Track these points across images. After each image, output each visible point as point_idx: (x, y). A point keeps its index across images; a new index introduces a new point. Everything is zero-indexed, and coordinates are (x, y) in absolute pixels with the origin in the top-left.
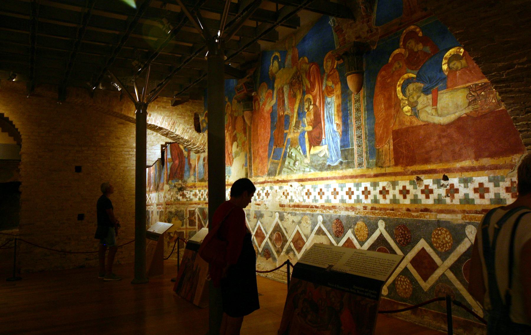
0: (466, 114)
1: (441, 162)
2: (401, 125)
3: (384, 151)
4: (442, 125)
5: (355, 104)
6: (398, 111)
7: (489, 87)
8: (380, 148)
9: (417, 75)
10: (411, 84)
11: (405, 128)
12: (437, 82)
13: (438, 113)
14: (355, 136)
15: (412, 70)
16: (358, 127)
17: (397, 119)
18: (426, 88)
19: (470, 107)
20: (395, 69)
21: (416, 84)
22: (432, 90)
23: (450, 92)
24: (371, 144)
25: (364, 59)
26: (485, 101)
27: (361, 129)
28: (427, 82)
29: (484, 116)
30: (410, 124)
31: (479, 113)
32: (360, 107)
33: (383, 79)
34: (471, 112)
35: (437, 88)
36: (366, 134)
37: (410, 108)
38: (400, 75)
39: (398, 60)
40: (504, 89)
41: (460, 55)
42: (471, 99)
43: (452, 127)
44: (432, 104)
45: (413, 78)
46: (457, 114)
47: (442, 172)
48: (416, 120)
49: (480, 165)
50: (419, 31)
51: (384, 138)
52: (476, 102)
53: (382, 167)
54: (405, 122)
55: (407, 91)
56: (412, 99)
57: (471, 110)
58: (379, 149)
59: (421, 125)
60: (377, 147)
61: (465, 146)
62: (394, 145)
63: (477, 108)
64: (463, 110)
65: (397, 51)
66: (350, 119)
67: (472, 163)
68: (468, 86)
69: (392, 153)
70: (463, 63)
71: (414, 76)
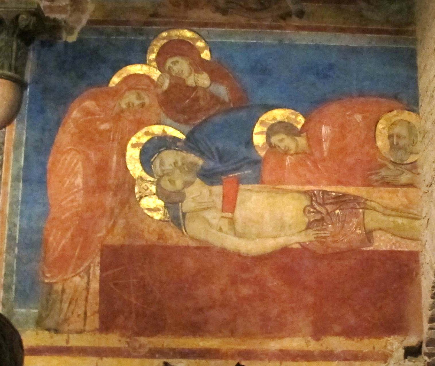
0: (301, 245)
3: (68, 291)
6: (123, 204)
7: (351, 205)
8: (56, 283)
9: (186, 136)
10: (170, 152)
12: (238, 165)
13: (234, 229)
15: (178, 121)
17: (121, 222)
19: (311, 232)
20: (129, 104)
21: (184, 154)
22: (223, 177)
23: (268, 192)
25: (31, 55)
26: (343, 227)
28: (213, 157)
29: (339, 255)
30: (158, 239)
33: (89, 118)
34: (311, 242)
37: (160, 203)
38: (140, 124)
39: (138, 89)
42: (312, 217)
44: (223, 208)
45: (175, 139)
46: (281, 241)
47: (232, 357)
48: (176, 232)
49: (324, 349)
50: (203, 49)
51: (74, 261)
52: (323, 225)
53: (57, 331)
54: (143, 231)
55: (157, 163)
56: (168, 183)
57: (312, 238)
58: (51, 285)
59: (188, 247)
60: (47, 277)
61: (292, 308)
62: (102, 281)
63: (325, 238)
64: (293, 235)
67: (306, 343)
68: (308, 191)
69: (94, 300)
71: (182, 137)
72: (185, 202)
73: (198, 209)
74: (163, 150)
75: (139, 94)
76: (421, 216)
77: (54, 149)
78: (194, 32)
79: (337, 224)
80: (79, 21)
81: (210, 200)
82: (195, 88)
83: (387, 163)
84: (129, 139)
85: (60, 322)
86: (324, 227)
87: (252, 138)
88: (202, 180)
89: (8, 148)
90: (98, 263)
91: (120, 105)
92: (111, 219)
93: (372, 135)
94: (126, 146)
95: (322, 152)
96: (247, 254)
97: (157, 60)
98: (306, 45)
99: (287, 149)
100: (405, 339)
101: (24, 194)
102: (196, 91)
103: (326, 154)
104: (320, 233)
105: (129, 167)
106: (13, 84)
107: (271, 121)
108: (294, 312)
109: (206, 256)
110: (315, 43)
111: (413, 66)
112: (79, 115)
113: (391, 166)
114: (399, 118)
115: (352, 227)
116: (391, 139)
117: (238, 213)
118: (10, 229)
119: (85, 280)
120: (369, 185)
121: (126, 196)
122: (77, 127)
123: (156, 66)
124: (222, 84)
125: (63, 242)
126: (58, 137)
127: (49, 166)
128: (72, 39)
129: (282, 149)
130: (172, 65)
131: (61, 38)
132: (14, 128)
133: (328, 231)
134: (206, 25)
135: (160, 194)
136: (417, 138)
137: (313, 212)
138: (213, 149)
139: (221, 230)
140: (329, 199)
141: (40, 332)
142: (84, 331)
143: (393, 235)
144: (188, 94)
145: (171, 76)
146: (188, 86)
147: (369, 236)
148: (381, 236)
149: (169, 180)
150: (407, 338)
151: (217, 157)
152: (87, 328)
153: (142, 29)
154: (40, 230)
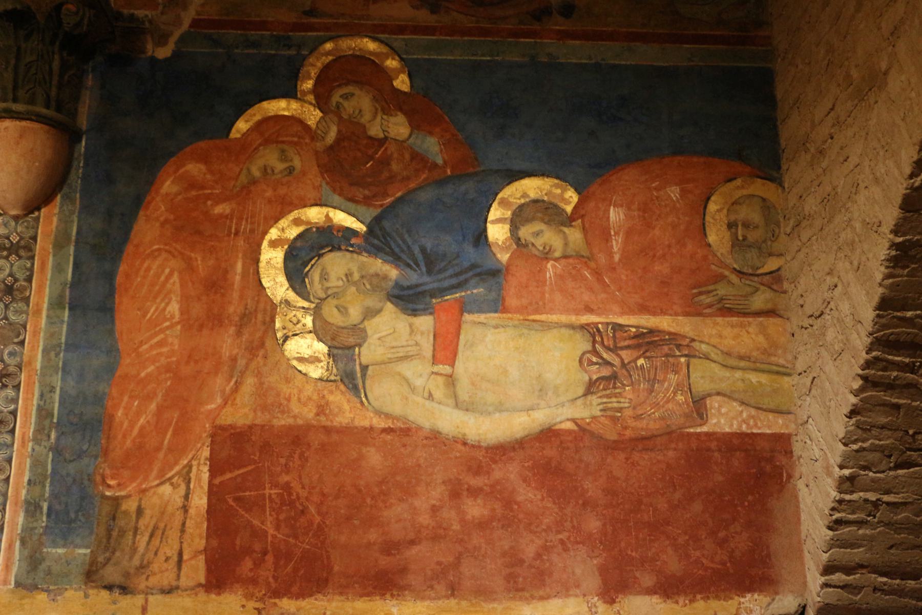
1: (453, 595)
2: (264, 408)
3: (148, 512)
4: (473, 446)
7: (666, 349)
8: (128, 496)
9: (367, 227)
11: (290, 428)
12: (462, 278)
13: (456, 396)
15: (352, 200)
17: (250, 382)
18: (409, 288)
19: (594, 399)
20: (265, 170)
21: (364, 258)
22: (434, 301)
23: (515, 326)
24: (72, 468)
26: (651, 391)
27: (17, 387)
28: (418, 265)
29: (644, 442)
30: (318, 414)
31: (626, 428)
32: (29, 279)
33: (194, 193)
34: (594, 418)
36: (44, 413)
37: (321, 348)
39: (283, 142)
40: (895, 374)
41: (563, 210)
42: (596, 372)
43: (511, 459)
44: (434, 356)
45: (350, 232)
46: (540, 418)
48: (348, 401)
51: (161, 455)
52: (615, 388)
53: (125, 590)
54: (289, 400)
55: (316, 275)
56: (335, 310)
58: (116, 501)
59: (372, 428)
61: (562, 542)
62: (214, 492)
63: (620, 410)
65: (280, 107)
67: (590, 609)
68: (588, 325)
72: (366, 345)
73: (390, 359)
74: (326, 250)
75: (283, 151)
76: (794, 368)
77: (129, 249)
78: (381, 41)
79: (639, 385)
80: (178, 22)
81: (410, 343)
82: (382, 142)
83: (727, 273)
84: (265, 233)
85: (132, 571)
86: (617, 391)
87: (485, 230)
88: (396, 305)
89: (43, 249)
90: (206, 459)
91: (249, 170)
92: (231, 377)
94: (259, 245)
95: (610, 255)
96: (479, 442)
97: (315, 91)
98: (576, 64)
99: (548, 248)
100: (773, 600)
102: (385, 146)
103: (617, 257)
105: (266, 283)
107: (519, 199)
108: (566, 550)
109: (404, 446)
110: (593, 61)
111: (771, 101)
112: (175, 189)
113: (734, 278)
114: (745, 192)
115: (667, 390)
116: (733, 230)
117: (462, 366)
118: (42, 396)
119: (182, 490)
120: (699, 314)
121: (258, 335)
123: (314, 102)
124: (431, 133)
125: (142, 421)
126: (136, 228)
127: (119, 279)
128: (163, 53)
129: (539, 250)
130: (341, 100)
131: (143, 52)
132: (56, 211)
133: (626, 398)
134: (401, 30)
136: (779, 227)
137: (596, 364)
138: (417, 251)
139: (430, 396)
140: (625, 339)
142: (177, 588)
143: (742, 403)
144: (370, 152)
145: (340, 118)
146: (370, 138)
147: (699, 406)
148: (720, 406)
150: (777, 598)
151: (422, 264)
152: (184, 582)
153: (289, 38)
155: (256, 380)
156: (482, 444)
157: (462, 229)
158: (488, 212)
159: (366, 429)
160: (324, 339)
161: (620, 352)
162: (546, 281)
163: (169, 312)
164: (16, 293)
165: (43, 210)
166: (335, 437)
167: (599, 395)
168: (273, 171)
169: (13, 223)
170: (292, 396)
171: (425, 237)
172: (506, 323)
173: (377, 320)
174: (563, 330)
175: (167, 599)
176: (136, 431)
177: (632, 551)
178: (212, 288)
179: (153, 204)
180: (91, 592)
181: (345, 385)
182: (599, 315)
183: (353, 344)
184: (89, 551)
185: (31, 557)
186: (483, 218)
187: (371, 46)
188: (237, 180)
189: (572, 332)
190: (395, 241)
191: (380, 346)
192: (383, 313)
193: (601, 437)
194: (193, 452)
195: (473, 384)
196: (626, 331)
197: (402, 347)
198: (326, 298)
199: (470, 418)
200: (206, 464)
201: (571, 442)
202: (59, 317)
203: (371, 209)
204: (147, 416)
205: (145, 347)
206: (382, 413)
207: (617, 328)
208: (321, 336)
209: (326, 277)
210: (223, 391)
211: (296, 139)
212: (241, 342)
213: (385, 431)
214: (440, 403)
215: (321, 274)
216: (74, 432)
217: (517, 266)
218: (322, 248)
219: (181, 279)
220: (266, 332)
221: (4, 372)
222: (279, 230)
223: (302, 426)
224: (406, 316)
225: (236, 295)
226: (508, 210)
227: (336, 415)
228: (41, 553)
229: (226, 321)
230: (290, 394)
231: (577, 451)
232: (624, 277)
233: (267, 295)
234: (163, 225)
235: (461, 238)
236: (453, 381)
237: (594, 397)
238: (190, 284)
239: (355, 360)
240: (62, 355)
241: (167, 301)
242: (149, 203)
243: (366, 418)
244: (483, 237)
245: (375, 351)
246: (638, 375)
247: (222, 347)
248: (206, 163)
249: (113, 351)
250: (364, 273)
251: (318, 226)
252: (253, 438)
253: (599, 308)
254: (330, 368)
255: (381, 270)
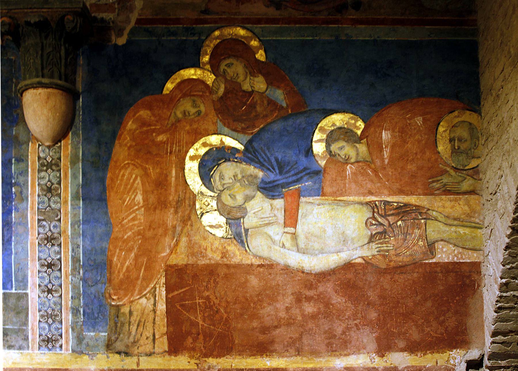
0: (364, 259)
2: (193, 254)
4: (307, 273)
5: (40, 171)
7: (413, 214)
9: (245, 146)
10: (229, 164)
11: (208, 265)
12: (299, 176)
13: (297, 245)
14: (32, 260)
16: (47, 239)
17: (184, 240)
18: (270, 183)
19: (374, 245)
21: (244, 166)
22: (284, 190)
24: (93, 290)
27: (60, 245)
28: (274, 169)
29: (401, 269)
30: (222, 258)
31: (391, 261)
32: (59, 183)
34: (373, 256)
35: (298, 190)
36: (76, 260)
37: (222, 220)
42: (375, 230)
44: (285, 223)
45: (235, 150)
48: (239, 250)
51: (139, 282)
52: (385, 238)
56: (229, 197)
59: (252, 265)
63: (388, 251)
66: (17, 210)
68: (370, 202)
70: (360, 150)
72: (247, 217)
73: (261, 225)
75: (194, 101)
76: (483, 225)
77: (112, 164)
79: (399, 236)
80: (128, 21)
81: (271, 215)
83: (448, 169)
84: (187, 152)
85: (130, 345)
86: (386, 240)
87: (312, 147)
88: (263, 193)
90: (163, 284)
91: (175, 113)
92: (174, 237)
93: (433, 139)
95: (383, 160)
96: (311, 271)
98: (363, 41)
99: (347, 157)
100: (467, 352)
101: (84, 213)
102: (253, 96)
103: (386, 161)
104: (383, 247)
106: (64, 94)
107: (331, 127)
108: (358, 329)
109: (270, 274)
110: (372, 38)
113: (452, 172)
114: (460, 119)
116: (453, 143)
118: (73, 250)
120: (432, 194)
121: (187, 212)
122: (133, 139)
123: (210, 69)
124: (279, 87)
126: (114, 151)
127: (108, 182)
129: (342, 158)
130: (226, 68)
131: (110, 41)
132: (70, 142)
133: (391, 244)
134: (259, 21)
135: (222, 209)
136: (479, 141)
137: (375, 225)
138: (273, 160)
140: (391, 210)
141: (111, 355)
142: (154, 353)
143: (455, 245)
146: (244, 91)
147: (431, 248)
148: (443, 248)
149: (229, 195)
150: (469, 351)
151: (276, 168)
152: (157, 350)
153: (193, 28)
154: (103, 251)
155: (187, 238)
156: (313, 272)
157: (298, 147)
158: (313, 135)
159: (249, 265)
160: (223, 214)
161: (388, 218)
162: (346, 176)
163: (137, 201)
164: (53, 191)
165: (62, 142)
166: (232, 270)
167: (377, 242)
168: (189, 114)
169: (48, 150)
170: (208, 247)
171: (277, 151)
172: (324, 202)
173: (252, 202)
174: (356, 206)
175: (149, 359)
176: (124, 269)
177: (394, 329)
178: (159, 185)
179: (123, 136)
180: (110, 355)
181: (236, 241)
182: (376, 196)
183: (240, 216)
184: (107, 334)
185: (78, 337)
186: (310, 139)
187: (242, 32)
188: (169, 120)
189: (361, 206)
190: (261, 155)
191: (255, 217)
192: (255, 198)
193: (377, 267)
194: (156, 280)
195: (307, 238)
196: (391, 205)
197: (267, 217)
198: (223, 190)
199: (305, 258)
200: (164, 287)
201: (361, 269)
202: (77, 205)
203: (246, 135)
204: (130, 260)
205: (125, 221)
206: (257, 256)
207: (386, 203)
208: (221, 212)
209: (223, 177)
210: (170, 246)
211: (201, 93)
212: (178, 217)
213: (259, 266)
214: (289, 250)
215: (220, 176)
216: (92, 270)
217: (330, 168)
218: (220, 160)
219: (142, 181)
220: (191, 211)
221: (52, 237)
222: (194, 150)
223: (214, 264)
224: (268, 200)
225: (173, 189)
226: (324, 134)
227: (232, 258)
228: (82, 335)
229: (169, 205)
230: (206, 246)
231: (364, 275)
232: (390, 173)
233: (190, 189)
234: (129, 148)
235: (298, 152)
236: (296, 237)
237: (374, 244)
238: (147, 184)
239: (241, 226)
240: (81, 227)
241: (135, 194)
242: (121, 135)
243: (249, 259)
244: (311, 151)
245: (252, 220)
246: (398, 231)
247: (167, 220)
248: (150, 110)
249: (108, 223)
250: (244, 175)
251: (216, 146)
252: (188, 271)
253: (376, 192)
254: (228, 231)
255: (253, 172)
